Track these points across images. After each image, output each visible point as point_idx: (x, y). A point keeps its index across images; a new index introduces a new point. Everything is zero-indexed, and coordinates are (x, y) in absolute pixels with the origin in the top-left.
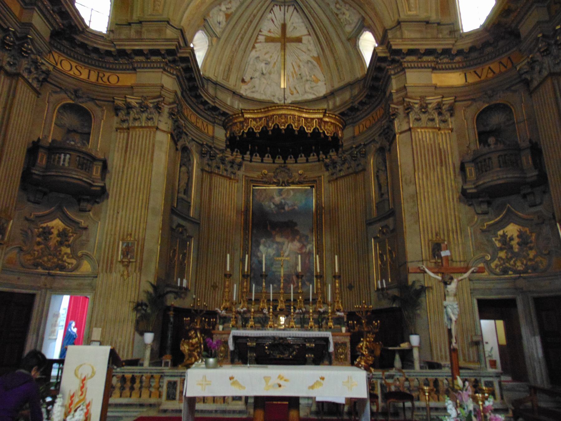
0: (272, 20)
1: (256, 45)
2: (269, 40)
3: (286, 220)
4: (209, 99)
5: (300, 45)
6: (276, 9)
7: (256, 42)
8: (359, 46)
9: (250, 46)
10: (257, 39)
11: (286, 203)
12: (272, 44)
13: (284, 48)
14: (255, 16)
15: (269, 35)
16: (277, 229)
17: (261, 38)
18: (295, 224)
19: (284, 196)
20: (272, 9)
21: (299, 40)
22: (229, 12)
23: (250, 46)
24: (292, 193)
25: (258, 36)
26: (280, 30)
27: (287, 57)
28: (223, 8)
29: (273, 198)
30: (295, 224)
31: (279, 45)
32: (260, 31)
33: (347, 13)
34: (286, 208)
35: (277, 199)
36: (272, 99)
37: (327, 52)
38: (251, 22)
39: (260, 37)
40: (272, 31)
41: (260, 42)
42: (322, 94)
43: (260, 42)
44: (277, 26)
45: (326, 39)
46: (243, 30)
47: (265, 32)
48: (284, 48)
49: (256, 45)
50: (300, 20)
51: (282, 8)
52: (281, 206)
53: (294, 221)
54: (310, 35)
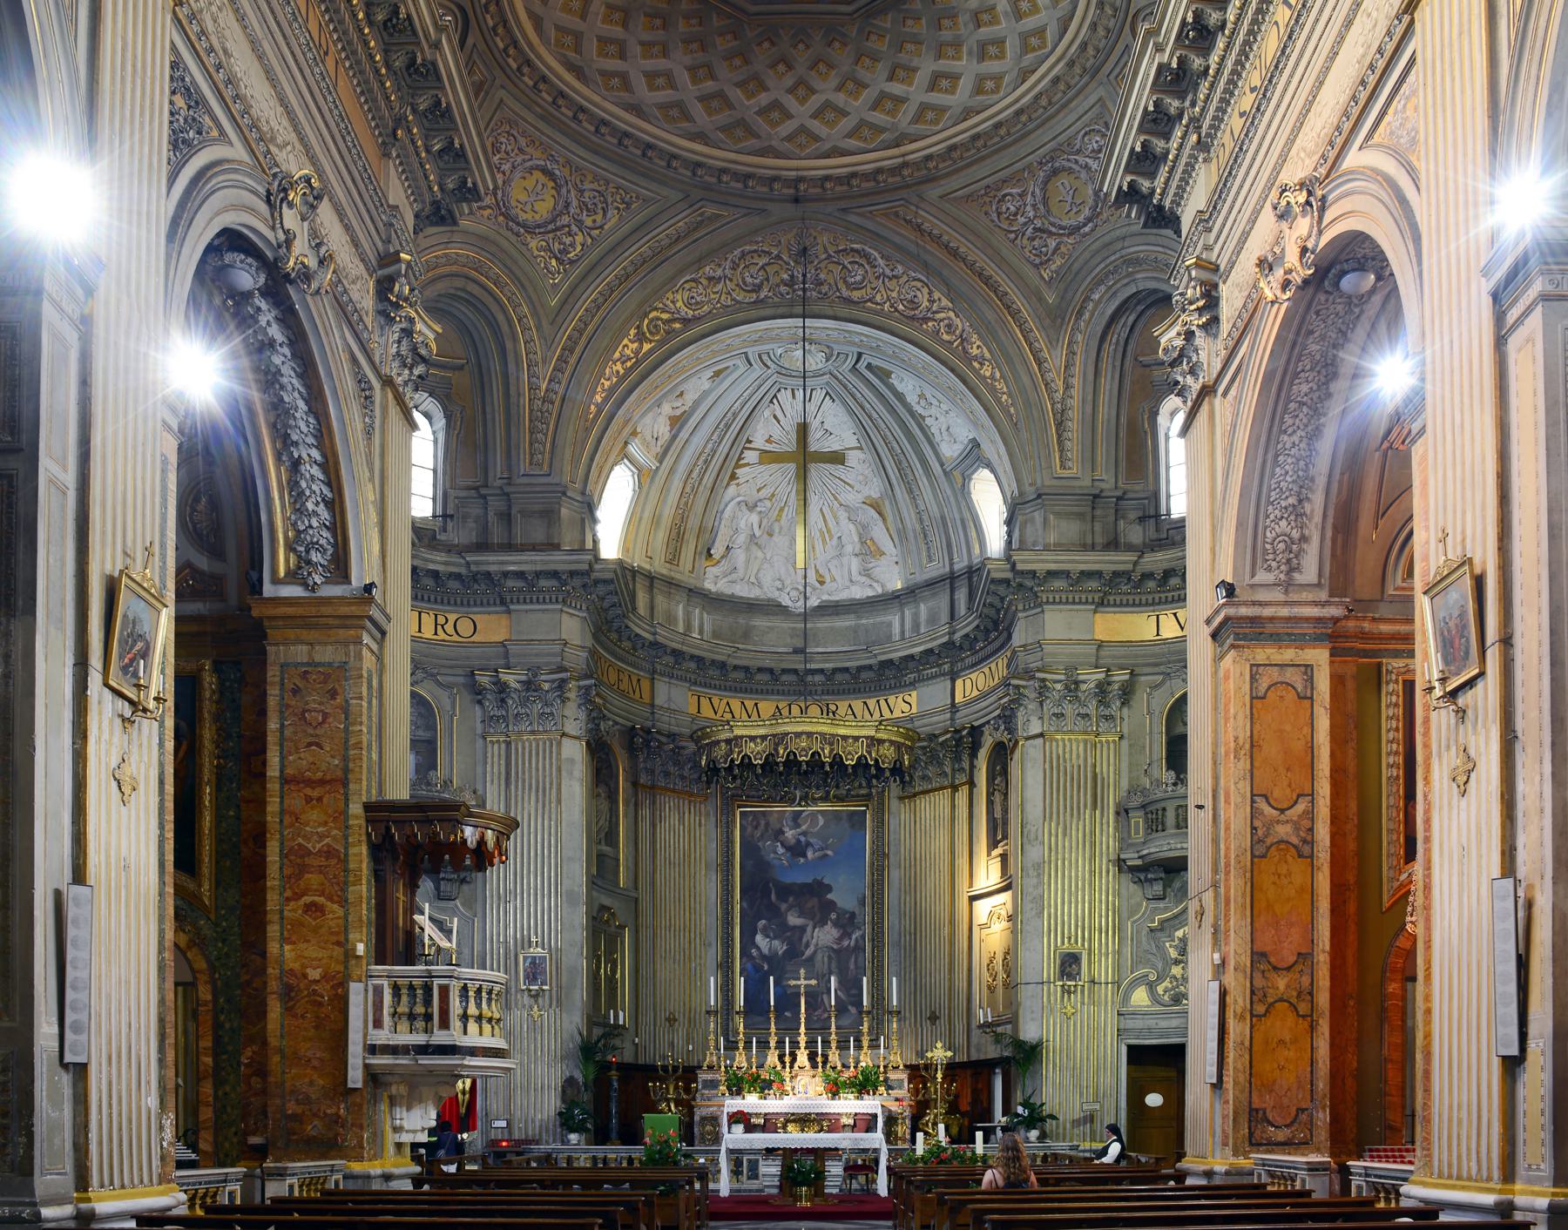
0: (775, 417)
1: (739, 472)
2: (768, 457)
3: (810, 881)
4: (644, 630)
5: (838, 470)
7: (737, 466)
8: (969, 493)
10: (740, 458)
12: (774, 466)
13: (803, 476)
14: (735, 415)
15: (769, 447)
16: (791, 899)
17: (750, 456)
18: (829, 889)
20: (775, 396)
21: (837, 458)
22: (678, 412)
25: (742, 452)
26: (794, 436)
27: (810, 495)
28: (666, 409)
30: (829, 889)
31: (791, 467)
32: (749, 441)
36: (775, 595)
37: (900, 492)
38: (728, 426)
39: (747, 453)
40: (776, 437)
41: (748, 464)
43: (748, 464)
44: (787, 428)
45: (898, 464)
46: (710, 446)
47: (759, 442)
48: (803, 476)
49: (739, 472)
53: (826, 881)
54: (861, 448)
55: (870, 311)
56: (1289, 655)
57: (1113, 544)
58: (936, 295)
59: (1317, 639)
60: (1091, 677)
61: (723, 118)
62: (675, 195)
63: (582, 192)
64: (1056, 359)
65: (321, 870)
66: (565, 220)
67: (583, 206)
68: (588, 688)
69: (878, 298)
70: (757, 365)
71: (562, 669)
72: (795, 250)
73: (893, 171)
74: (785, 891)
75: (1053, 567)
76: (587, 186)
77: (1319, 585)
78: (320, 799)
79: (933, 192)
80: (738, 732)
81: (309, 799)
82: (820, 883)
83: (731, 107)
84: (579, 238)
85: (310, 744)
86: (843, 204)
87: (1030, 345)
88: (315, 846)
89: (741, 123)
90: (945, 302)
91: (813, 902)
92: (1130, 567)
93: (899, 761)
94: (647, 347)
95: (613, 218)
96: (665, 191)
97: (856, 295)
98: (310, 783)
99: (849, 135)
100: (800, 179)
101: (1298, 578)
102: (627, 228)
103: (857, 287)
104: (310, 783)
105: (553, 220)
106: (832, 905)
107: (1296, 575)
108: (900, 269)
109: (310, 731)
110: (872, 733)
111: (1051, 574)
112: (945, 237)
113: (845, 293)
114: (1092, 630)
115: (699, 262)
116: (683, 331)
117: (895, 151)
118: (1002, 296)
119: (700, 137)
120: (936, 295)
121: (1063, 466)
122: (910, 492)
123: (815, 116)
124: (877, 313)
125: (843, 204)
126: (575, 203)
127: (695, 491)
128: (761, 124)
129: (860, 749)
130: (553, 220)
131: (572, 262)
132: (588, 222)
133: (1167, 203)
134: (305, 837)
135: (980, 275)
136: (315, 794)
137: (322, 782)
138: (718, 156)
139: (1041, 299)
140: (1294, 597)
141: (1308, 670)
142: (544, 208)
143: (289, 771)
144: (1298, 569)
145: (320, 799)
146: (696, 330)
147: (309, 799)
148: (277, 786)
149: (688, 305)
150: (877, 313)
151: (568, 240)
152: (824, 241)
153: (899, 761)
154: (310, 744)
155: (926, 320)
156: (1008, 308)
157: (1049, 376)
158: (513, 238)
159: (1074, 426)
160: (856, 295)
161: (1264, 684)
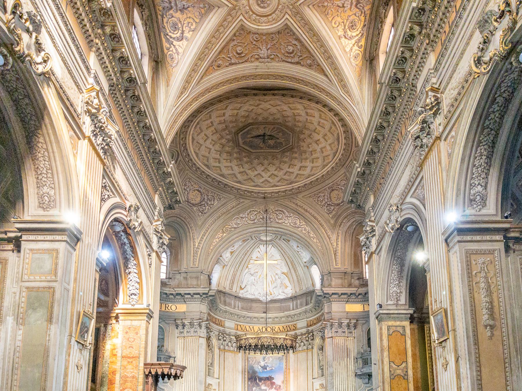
3: (268, 376)
6: (261, 246)
9: (245, 266)
11: (267, 366)
14: (248, 251)
19: (266, 361)
23: (245, 266)
24: (271, 359)
29: (260, 362)
33: (304, 253)
34: (268, 368)
35: (262, 364)
37: (292, 271)
42: (289, 296)
50: (276, 252)
51: (265, 246)
52: (264, 368)
55: (284, 225)
56: (398, 323)
57: (350, 285)
58: (301, 221)
59: (406, 319)
60: (346, 322)
61: (245, 177)
62: (233, 197)
63: (208, 196)
64: (334, 237)
65: (131, 382)
66: (203, 203)
67: (208, 199)
68: (207, 324)
69: (286, 222)
70: (254, 238)
71: (200, 319)
72: (264, 210)
73: (290, 190)
74: (261, 379)
75: (334, 292)
76: (209, 194)
77: (406, 304)
78: (132, 362)
79: (300, 196)
80: (248, 336)
81: (129, 362)
82: (271, 377)
83: (247, 175)
84: (207, 207)
85: (130, 347)
86: (276, 199)
87: (327, 234)
88: (129, 375)
89: (250, 179)
90: (304, 223)
91: (269, 382)
92: (355, 292)
93: (292, 344)
94: (225, 234)
95: (216, 202)
96: (230, 196)
97: (280, 221)
98: (129, 358)
99: (278, 182)
100: (265, 193)
101: (400, 302)
102: (220, 205)
103: (281, 219)
104: (129, 358)
105: (200, 203)
106: (274, 383)
107: (399, 302)
108: (292, 215)
109: (130, 343)
110: (284, 337)
111: (333, 294)
112: (304, 207)
113: (277, 221)
114: (345, 308)
115: (239, 213)
116: (234, 231)
117: (290, 186)
118: (319, 222)
119: (239, 182)
120: (301, 221)
121: (336, 265)
122: (295, 271)
123: (269, 177)
124: (285, 226)
125: (276, 199)
126: (206, 198)
127: (237, 270)
128: (255, 179)
129: (282, 341)
130: (200, 203)
131: (205, 213)
132: (210, 203)
133: (361, 204)
134: (127, 373)
135: (313, 216)
136: (130, 360)
137: (133, 357)
138: (244, 187)
139: (329, 222)
140: (399, 308)
141: (404, 327)
142: (198, 200)
143: (124, 354)
144: (399, 300)
145: (132, 362)
146: (238, 230)
147: (129, 362)
148: (120, 359)
149: (236, 224)
150: (285, 226)
151: (204, 208)
152: (271, 207)
153: (292, 344)
154: (130, 347)
155: (298, 227)
156: (321, 224)
157: (332, 242)
158: (190, 207)
159: (339, 254)
160: (280, 221)
161: (391, 331)
